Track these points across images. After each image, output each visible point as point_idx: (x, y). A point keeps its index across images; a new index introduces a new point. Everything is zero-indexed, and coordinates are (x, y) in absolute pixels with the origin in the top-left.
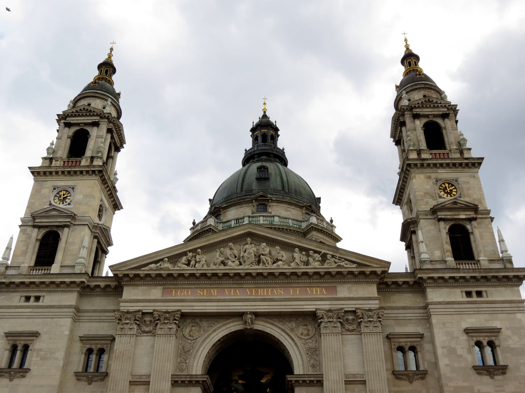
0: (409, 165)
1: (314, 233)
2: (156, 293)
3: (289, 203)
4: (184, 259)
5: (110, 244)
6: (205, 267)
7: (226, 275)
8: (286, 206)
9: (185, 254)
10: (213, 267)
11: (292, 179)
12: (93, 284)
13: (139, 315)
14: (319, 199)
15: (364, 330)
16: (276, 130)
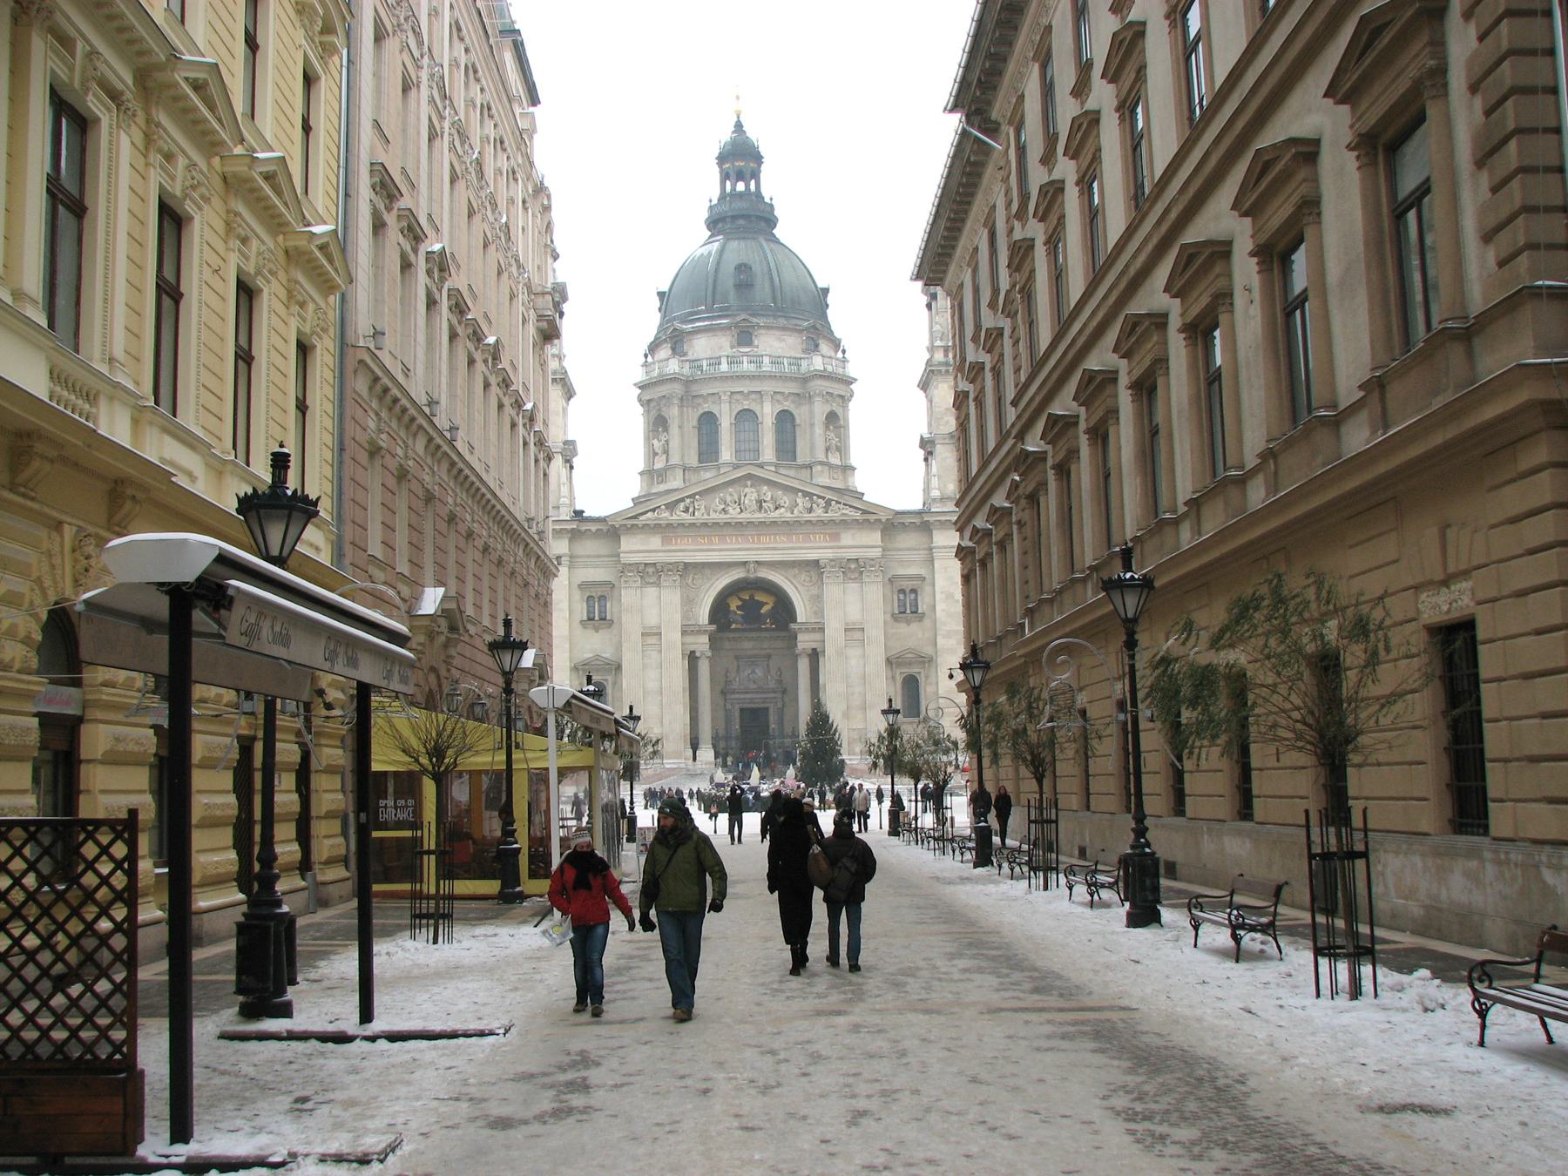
0: (932, 371)
1: (819, 382)
2: (655, 542)
3: (784, 329)
4: (682, 506)
5: (574, 453)
6: (706, 517)
7: (727, 524)
8: (777, 333)
9: (682, 500)
10: (713, 515)
11: (788, 276)
12: (583, 528)
13: (643, 566)
14: (826, 291)
15: (865, 579)
16: (758, 159)
